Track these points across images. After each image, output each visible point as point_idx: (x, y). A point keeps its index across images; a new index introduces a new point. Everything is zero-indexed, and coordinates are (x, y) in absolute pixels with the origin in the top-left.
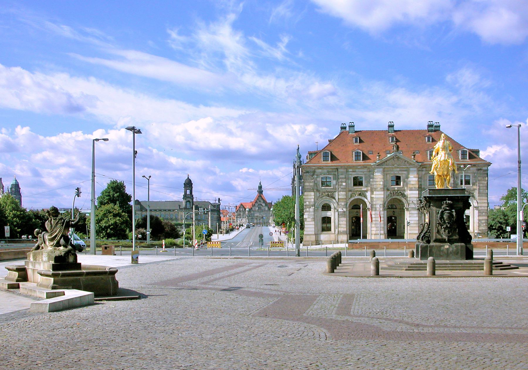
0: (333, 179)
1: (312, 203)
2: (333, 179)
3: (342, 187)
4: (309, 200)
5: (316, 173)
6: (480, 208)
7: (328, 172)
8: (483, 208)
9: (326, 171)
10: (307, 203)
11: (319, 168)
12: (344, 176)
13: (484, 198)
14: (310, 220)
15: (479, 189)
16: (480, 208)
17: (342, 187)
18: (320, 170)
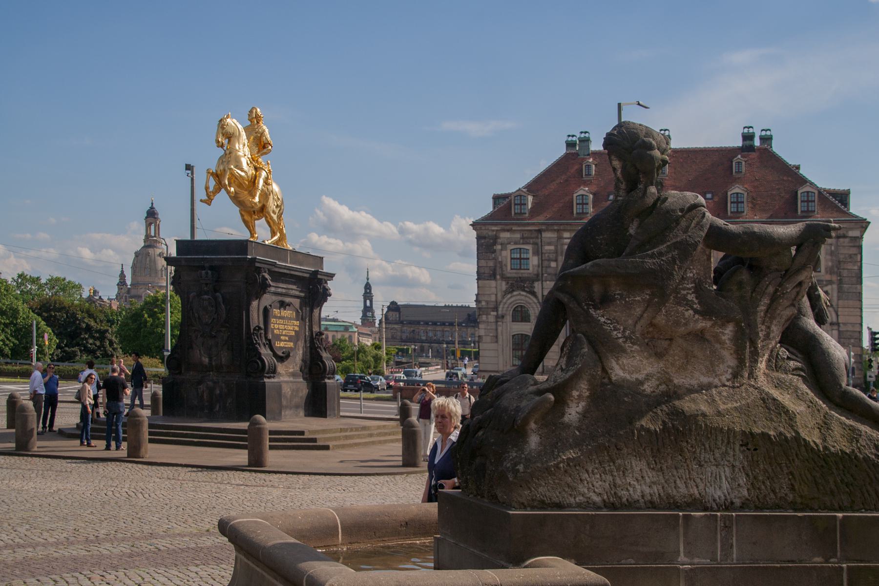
0: (534, 254)
1: (492, 305)
2: (534, 254)
3: (549, 270)
4: (486, 298)
5: (499, 241)
6: (842, 328)
7: (523, 238)
8: (850, 328)
9: (518, 236)
10: (483, 303)
11: (504, 230)
12: (552, 248)
13: (851, 303)
14: (488, 339)
15: (840, 282)
16: (842, 328)
17: (549, 270)
18: (507, 235)
